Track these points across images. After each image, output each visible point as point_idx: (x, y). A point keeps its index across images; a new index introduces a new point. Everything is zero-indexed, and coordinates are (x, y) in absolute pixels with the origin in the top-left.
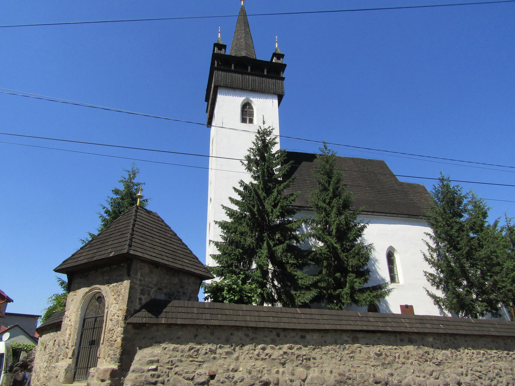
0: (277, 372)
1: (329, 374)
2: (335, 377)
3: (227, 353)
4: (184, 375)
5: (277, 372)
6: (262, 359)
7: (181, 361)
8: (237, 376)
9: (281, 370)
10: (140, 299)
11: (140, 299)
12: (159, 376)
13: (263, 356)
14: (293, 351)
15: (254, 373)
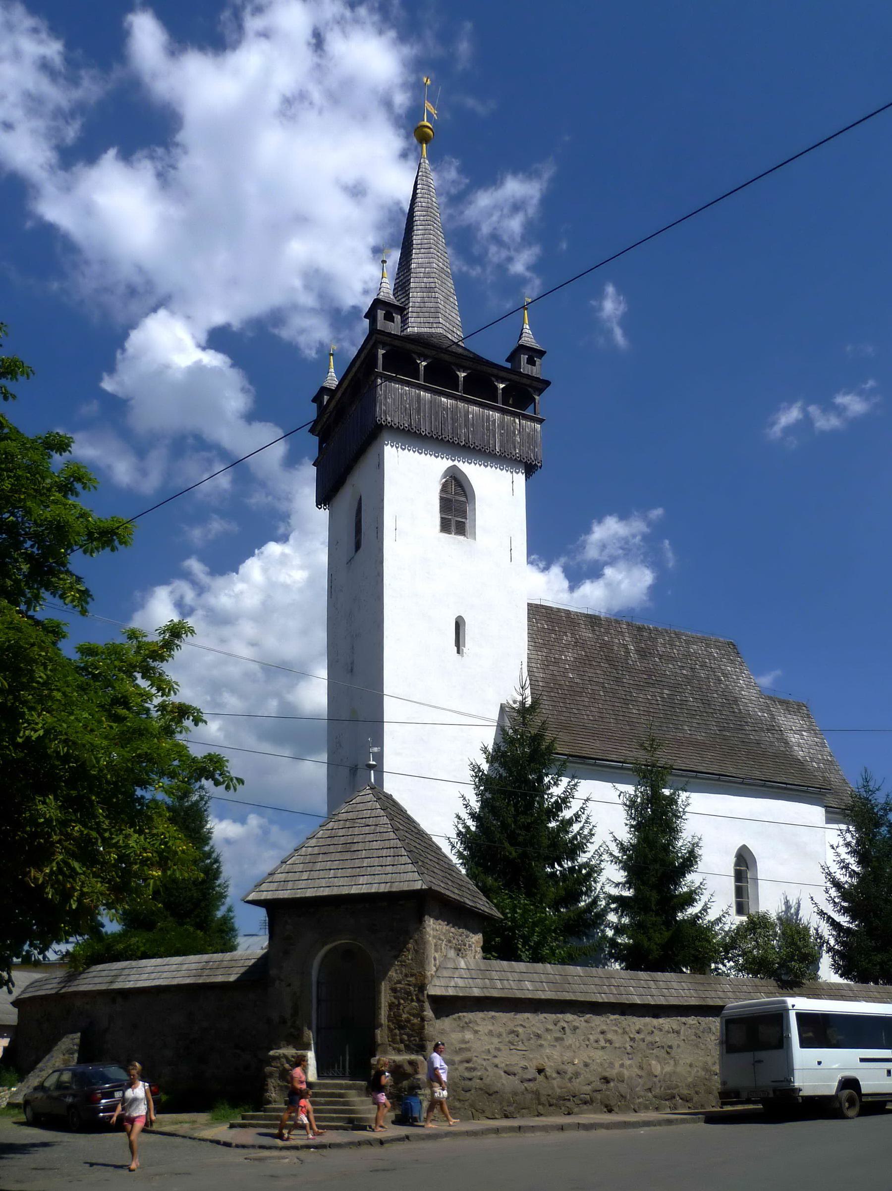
0: (622, 1065)
1: (689, 1069)
2: (698, 1071)
3: (557, 1039)
4: (506, 1069)
5: (622, 1065)
6: (603, 1048)
7: (499, 1050)
8: (570, 1069)
9: (628, 1062)
10: (435, 959)
11: (435, 959)
12: (474, 1069)
13: (602, 1043)
14: (641, 1036)
15: (593, 1067)
